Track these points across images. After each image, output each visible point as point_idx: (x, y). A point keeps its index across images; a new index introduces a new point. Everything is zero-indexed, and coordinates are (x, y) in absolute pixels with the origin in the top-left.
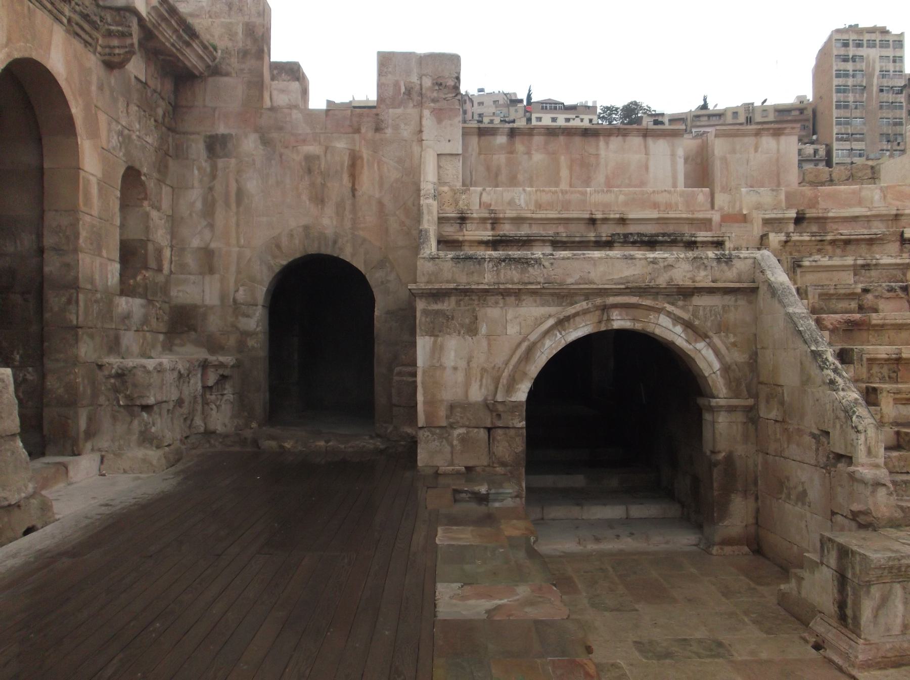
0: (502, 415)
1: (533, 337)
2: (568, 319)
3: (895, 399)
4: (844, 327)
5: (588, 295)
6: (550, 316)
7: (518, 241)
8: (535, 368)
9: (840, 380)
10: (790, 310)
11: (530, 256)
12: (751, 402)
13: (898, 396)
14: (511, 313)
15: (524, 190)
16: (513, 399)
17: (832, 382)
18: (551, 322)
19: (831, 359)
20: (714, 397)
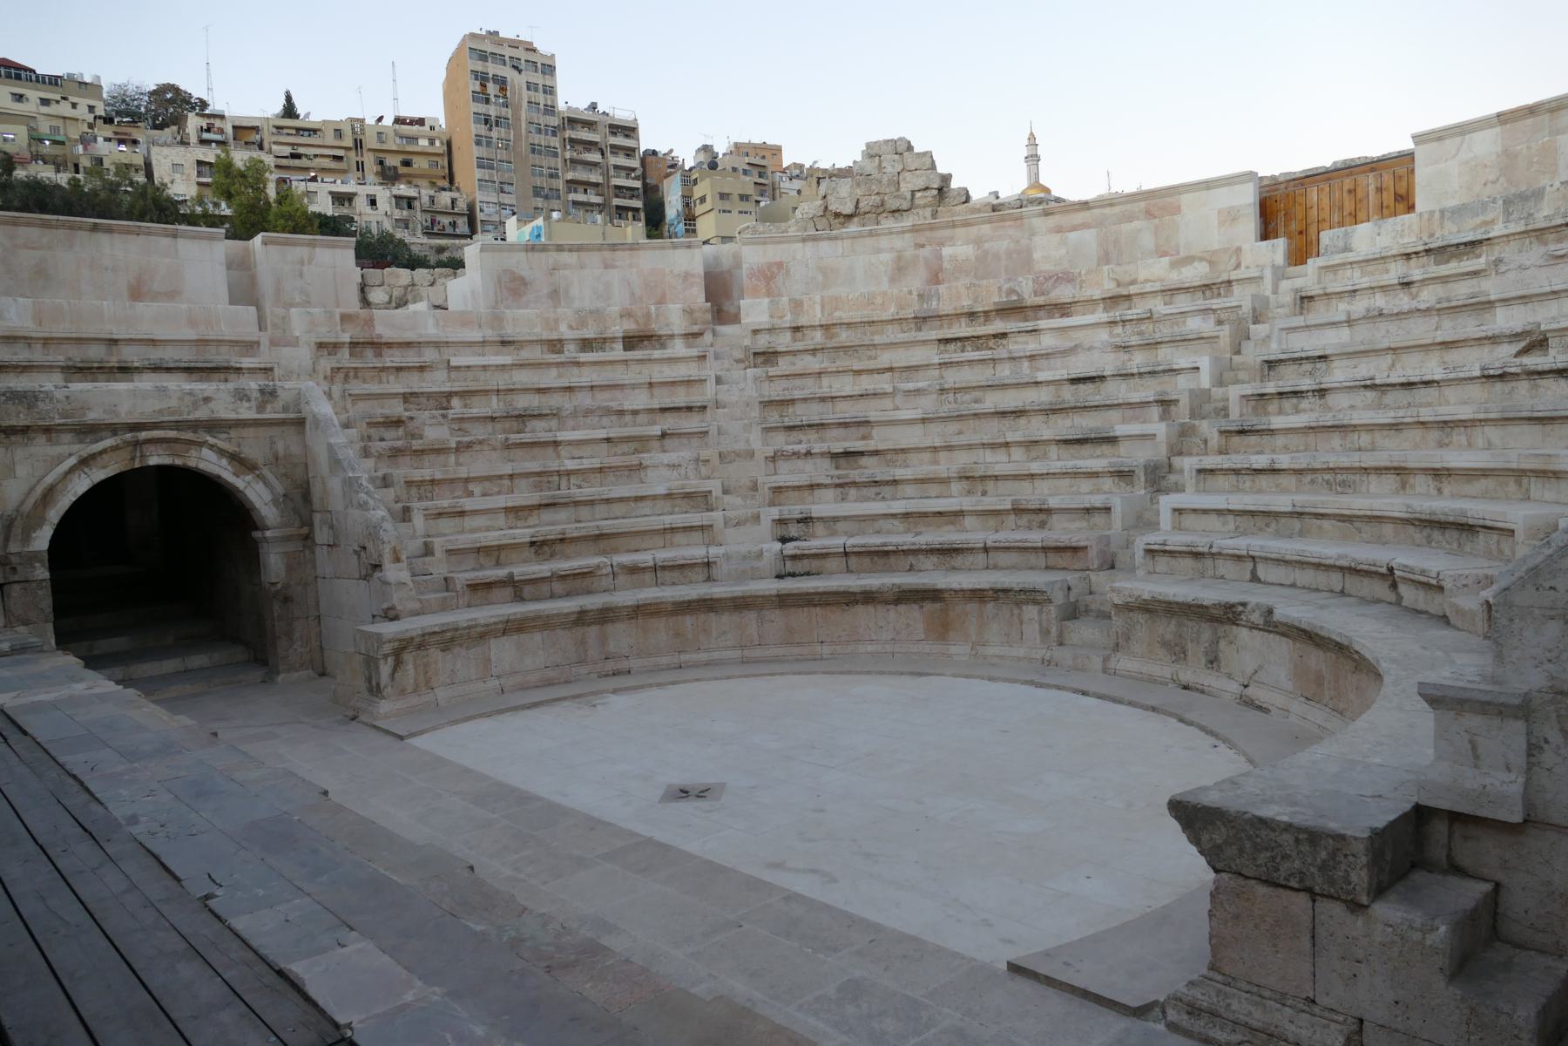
0: (19, 568)
1: (49, 479)
2: (93, 457)
3: (425, 515)
4: (390, 453)
5: (114, 429)
6: (70, 455)
7: (17, 367)
8: (55, 514)
9: (371, 502)
10: (332, 440)
11: (37, 389)
12: (305, 530)
13: (426, 512)
14: (20, 453)
15: (15, 300)
16: (31, 549)
17: (366, 503)
18: (72, 461)
19: (365, 483)
20: (257, 529)
